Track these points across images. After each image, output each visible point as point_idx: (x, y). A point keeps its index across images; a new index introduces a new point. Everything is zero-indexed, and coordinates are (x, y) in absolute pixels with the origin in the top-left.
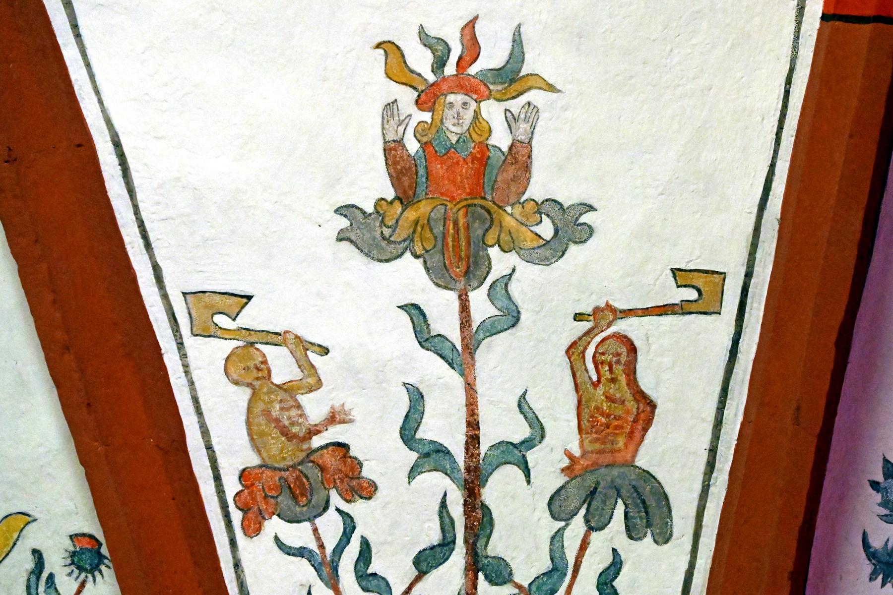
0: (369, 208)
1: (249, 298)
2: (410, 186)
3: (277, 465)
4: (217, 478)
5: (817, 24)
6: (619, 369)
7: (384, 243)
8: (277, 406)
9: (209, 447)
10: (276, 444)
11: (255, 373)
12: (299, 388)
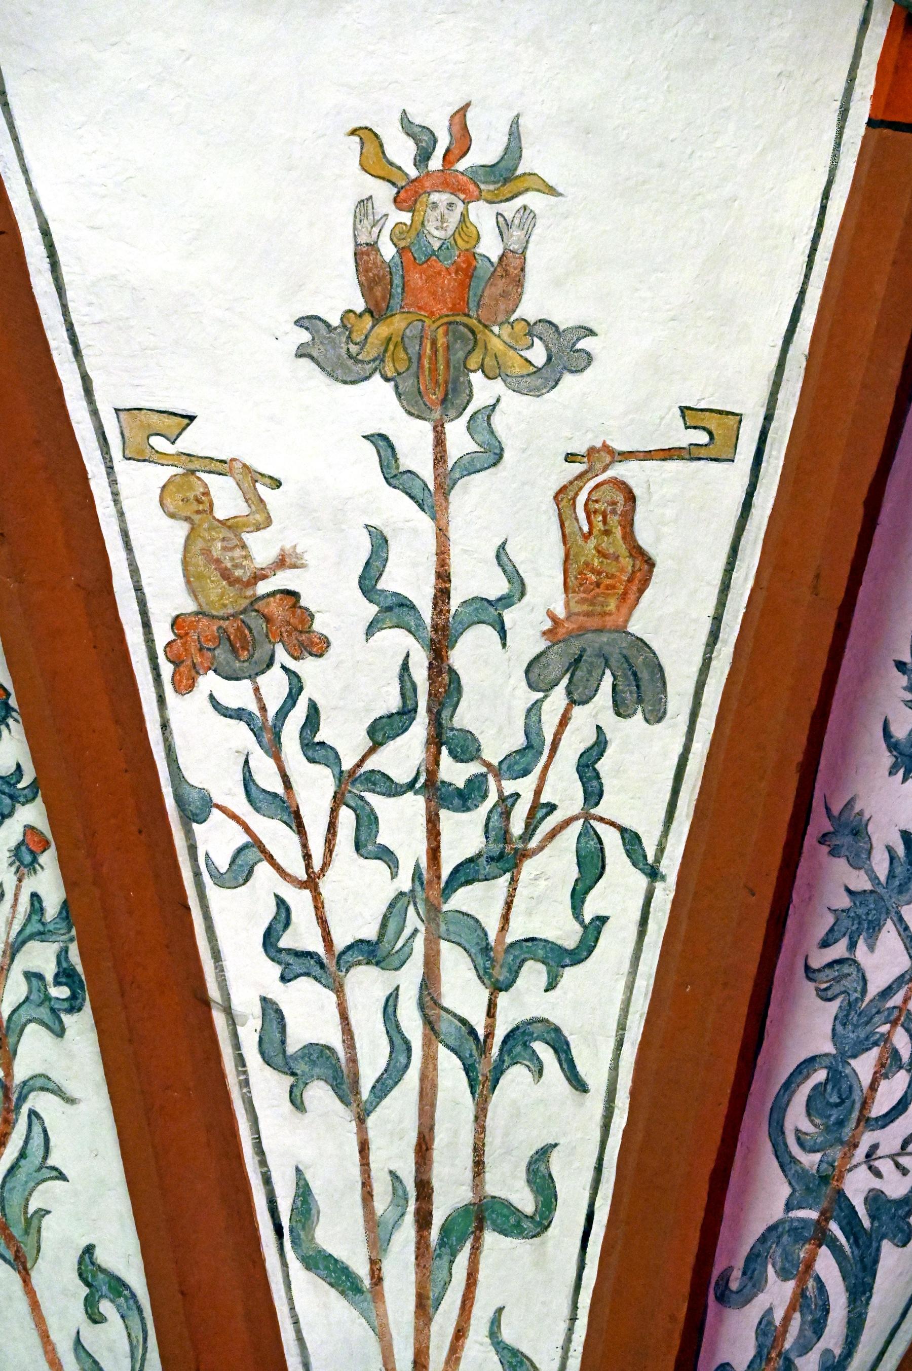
0: (335, 321)
1: (192, 418)
2: (384, 298)
3: (215, 613)
4: (146, 625)
5: (862, 130)
6: (613, 520)
7: (350, 362)
8: (219, 545)
9: (138, 589)
10: (216, 588)
11: (195, 506)
12: (244, 525)
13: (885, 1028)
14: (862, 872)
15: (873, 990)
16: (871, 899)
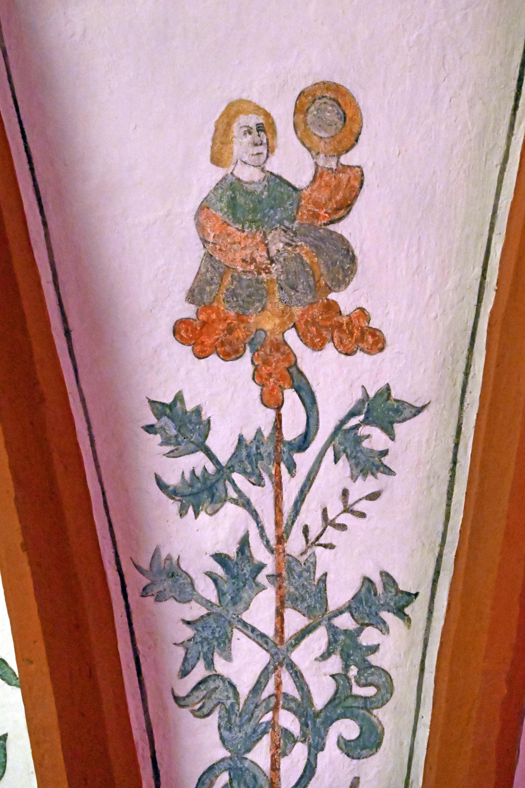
13: (268, 717)
14: (193, 603)
15: (244, 690)
16: (211, 620)
